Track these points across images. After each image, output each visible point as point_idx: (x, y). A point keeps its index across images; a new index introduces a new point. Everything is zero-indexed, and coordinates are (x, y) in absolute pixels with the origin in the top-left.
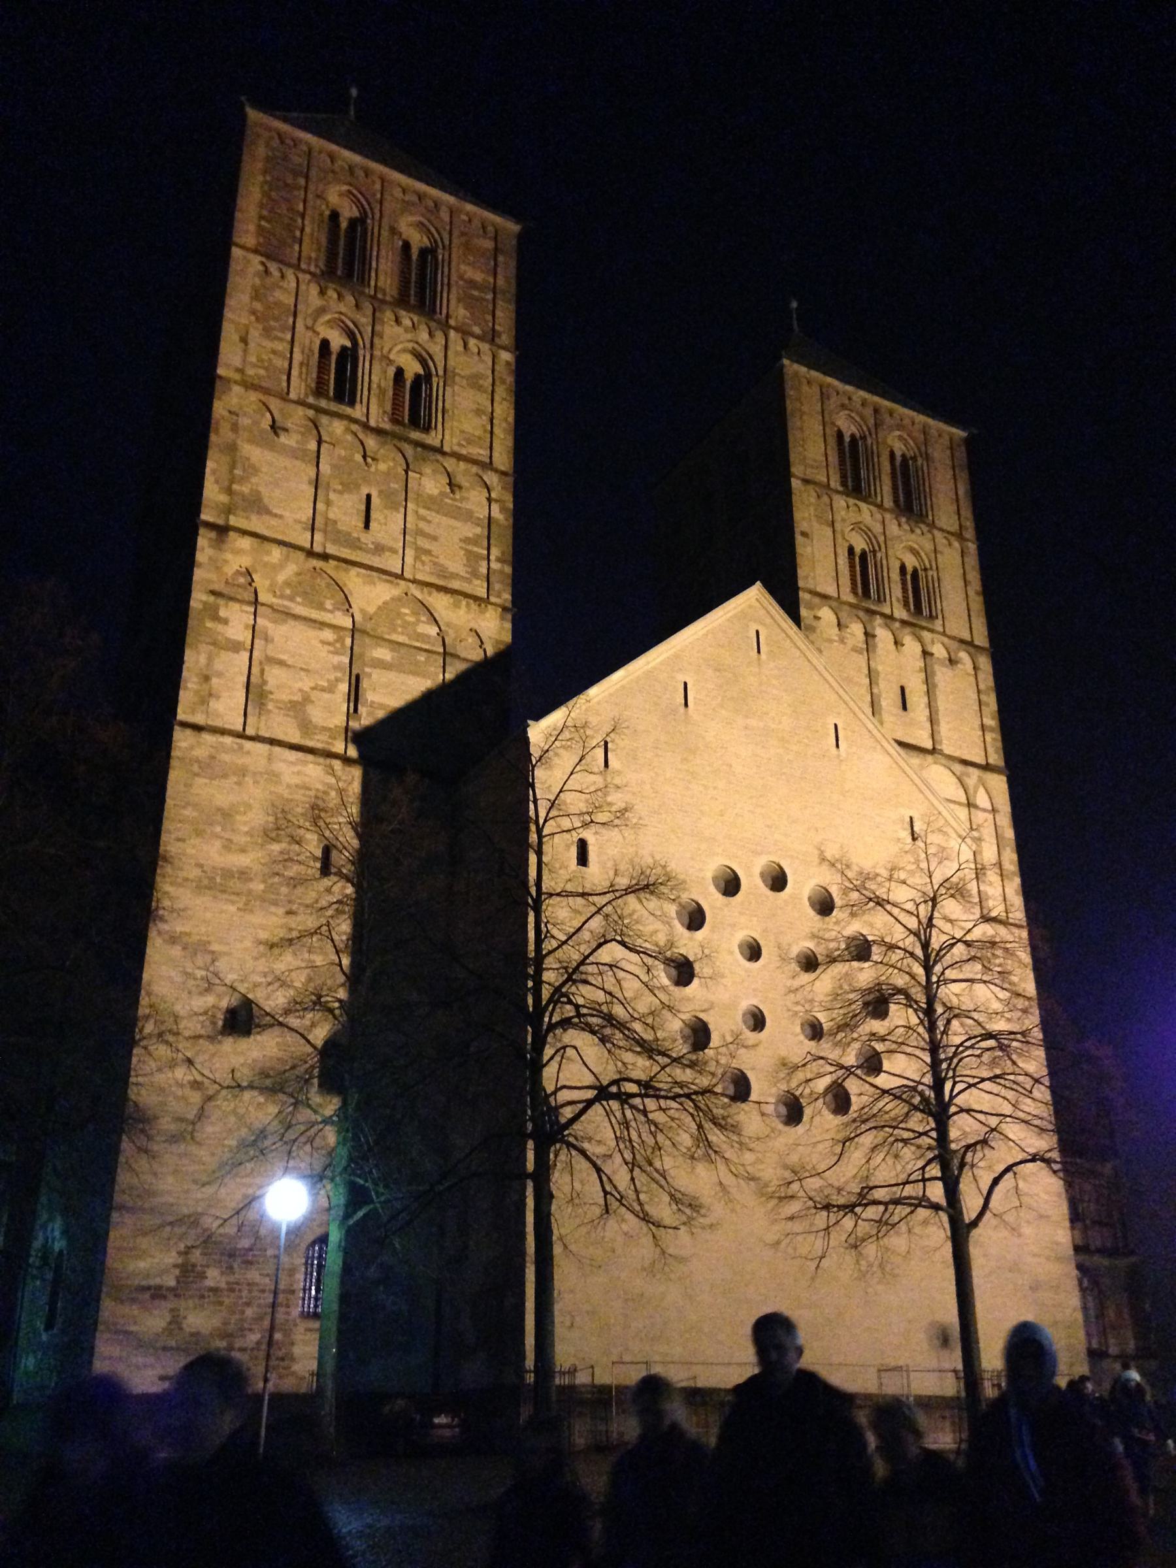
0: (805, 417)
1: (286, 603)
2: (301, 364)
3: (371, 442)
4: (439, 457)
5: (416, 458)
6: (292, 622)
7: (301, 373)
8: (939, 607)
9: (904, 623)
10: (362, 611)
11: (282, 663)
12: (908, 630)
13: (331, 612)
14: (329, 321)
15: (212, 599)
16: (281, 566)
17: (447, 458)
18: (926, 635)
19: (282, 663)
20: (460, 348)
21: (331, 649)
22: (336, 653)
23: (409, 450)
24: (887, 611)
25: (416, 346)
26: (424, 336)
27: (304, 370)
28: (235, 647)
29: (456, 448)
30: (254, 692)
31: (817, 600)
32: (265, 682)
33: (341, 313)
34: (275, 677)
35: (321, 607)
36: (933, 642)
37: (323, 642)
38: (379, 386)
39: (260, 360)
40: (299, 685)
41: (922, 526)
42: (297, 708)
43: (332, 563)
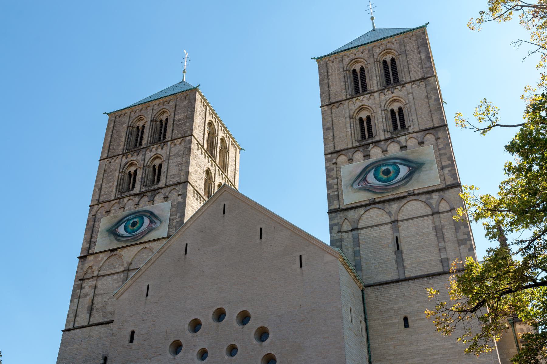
0: (330, 77)
1: (104, 272)
2: (117, 186)
3: (137, 199)
4: (160, 190)
5: (152, 196)
6: (105, 278)
7: (117, 188)
8: (411, 120)
9: (386, 140)
10: (127, 262)
11: (99, 294)
12: (390, 141)
13: (118, 267)
14: (130, 165)
15: (79, 282)
16: (103, 258)
17: (163, 189)
18: (402, 139)
19: (99, 294)
20: (172, 146)
21: (116, 281)
22: (118, 282)
23: (149, 194)
24: (377, 139)
25: (157, 155)
26: (160, 149)
27: (118, 187)
28: (86, 295)
29: (168, 184)
30: (91, 309)
31: (335, 155)
32: (93, 304)
33: (132, 160)
34: (98, 299)
35: (115, 268)
36: (406, 140)
37: (114, 280)
38: (142, 177)
39: (105, 192)
40: (104, 300)
41: (399, 87)
42: (103, 308)
43: (118, 250)
